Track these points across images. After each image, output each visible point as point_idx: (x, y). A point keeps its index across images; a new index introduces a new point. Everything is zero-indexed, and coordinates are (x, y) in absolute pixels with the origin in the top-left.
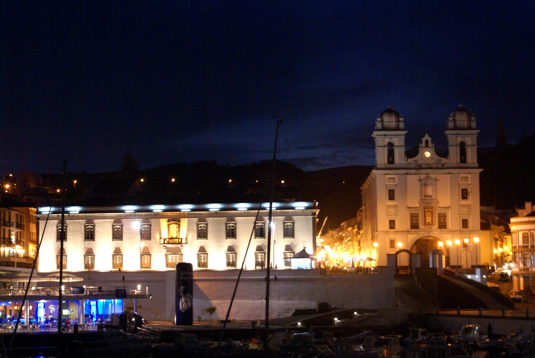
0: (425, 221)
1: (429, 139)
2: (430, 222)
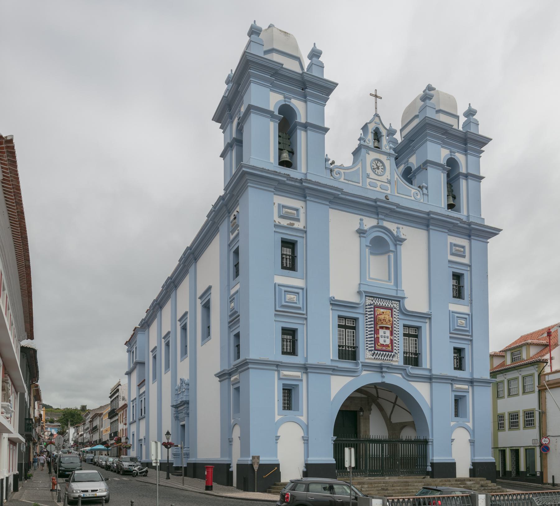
0: (376, 340)
2: (387, 346)
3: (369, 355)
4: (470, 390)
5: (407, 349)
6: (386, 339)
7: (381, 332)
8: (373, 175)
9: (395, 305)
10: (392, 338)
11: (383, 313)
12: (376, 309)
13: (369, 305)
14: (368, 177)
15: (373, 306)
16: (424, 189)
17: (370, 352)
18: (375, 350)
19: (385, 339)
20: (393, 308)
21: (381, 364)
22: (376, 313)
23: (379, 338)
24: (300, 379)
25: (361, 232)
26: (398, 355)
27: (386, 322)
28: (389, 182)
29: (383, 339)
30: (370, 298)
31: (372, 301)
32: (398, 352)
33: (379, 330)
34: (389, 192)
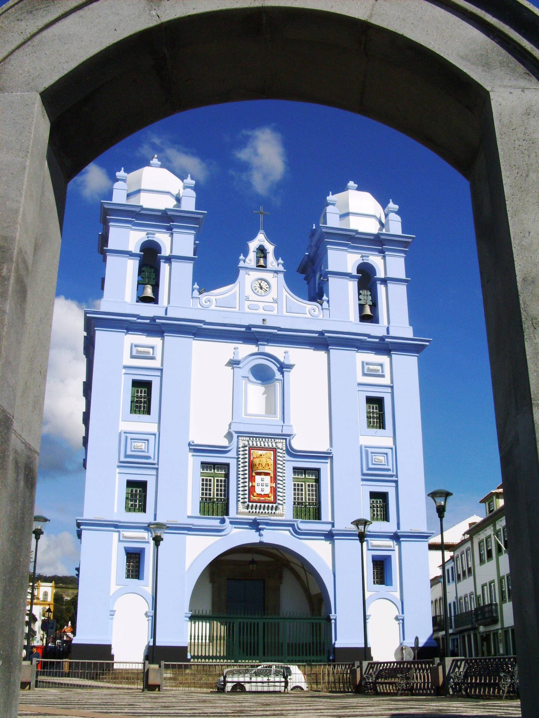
0: (252, 490)
1: (270, 248)
3: (241, 508)
4: (397, 548)
5: (302, 499)
6: (264, 487)
7: (258, 478)
8: (253, 297)
9: (280, 445)
10: (274, 485)
11: (261, 455)
12: (252, 451)
13: (242, 447)
14: (247, 299)
15: (247, 448)
16: (325, 304)
17: (243, 504)
18: (250, 501)
19: (263, 487)
20: (276, 449)
21: (255, 520)
22: (252, 456)
23: (255, 486)
24: (147, 540)
25: (234, 363)
26: (284, 506)
27: (263, 467)
28: (275, 301)
29: (260, 487)
30: (245, 438)
31: (248, 441)
32: (284, 503)
33: (254, 477)
34: (275, 312)
